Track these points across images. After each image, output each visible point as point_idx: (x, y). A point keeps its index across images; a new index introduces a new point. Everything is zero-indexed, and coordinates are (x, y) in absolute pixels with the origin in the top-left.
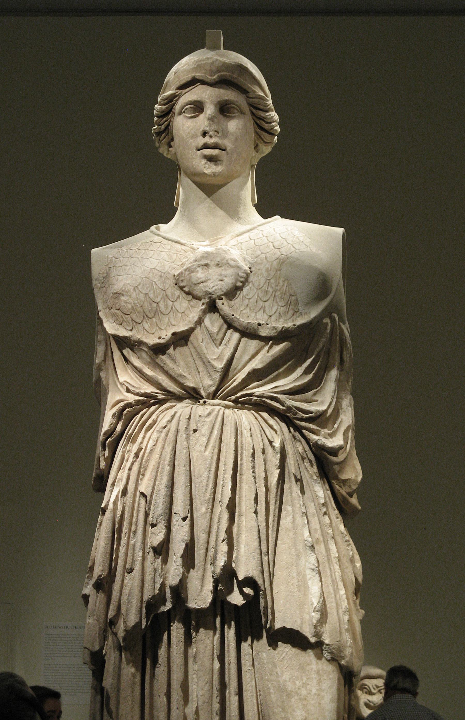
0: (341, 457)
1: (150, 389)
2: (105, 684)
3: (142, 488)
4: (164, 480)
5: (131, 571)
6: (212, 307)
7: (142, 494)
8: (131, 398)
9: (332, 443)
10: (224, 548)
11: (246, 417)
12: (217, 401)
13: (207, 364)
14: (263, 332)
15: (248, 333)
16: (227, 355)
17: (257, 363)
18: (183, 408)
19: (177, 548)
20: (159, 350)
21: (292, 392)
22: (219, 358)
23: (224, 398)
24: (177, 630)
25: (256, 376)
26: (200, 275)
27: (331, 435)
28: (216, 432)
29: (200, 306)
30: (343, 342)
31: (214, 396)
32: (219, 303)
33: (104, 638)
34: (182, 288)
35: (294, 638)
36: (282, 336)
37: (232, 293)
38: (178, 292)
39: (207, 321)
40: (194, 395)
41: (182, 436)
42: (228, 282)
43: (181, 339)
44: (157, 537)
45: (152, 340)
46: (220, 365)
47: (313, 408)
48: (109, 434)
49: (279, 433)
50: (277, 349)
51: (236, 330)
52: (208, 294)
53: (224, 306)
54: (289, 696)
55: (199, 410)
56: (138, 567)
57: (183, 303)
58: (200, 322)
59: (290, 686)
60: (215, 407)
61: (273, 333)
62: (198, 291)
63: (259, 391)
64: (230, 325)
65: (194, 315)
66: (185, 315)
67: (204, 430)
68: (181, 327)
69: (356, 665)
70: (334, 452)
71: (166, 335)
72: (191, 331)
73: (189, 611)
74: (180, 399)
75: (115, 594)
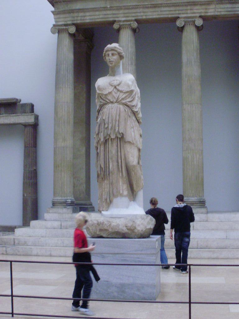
0: (138, 112)
1: (105, 102)
2: (98, 151)
3: (103, 118)
4: (107, 117)
5: (102, 132)
6: (115, 87)
7: (104, 119)
8: (102, 103)
9: (136, 110)
10: (117, 128)
11: (121, 106)
12: (116, 103)
13: (115, 98)
14: (124, 91)
15: (121, 92)
16: (118, 96)
17: (123, 97)
18: (110, 105)
19: (110, 128)
20: (106, 95)
21: (129, 102)
22: (116, 96)
23: (118, 103)
24: (110, 142)
25: (123, 99)
26: (113, 82)
27: (136, 109)
28: (116, 109)
29: (113, 88)
30: (138, 93)
31: (116, 102)
32: (116, 87)
33: (98, 144)
34: (110, 85)
35: (129, 142)
36: (127, 92)
37: (119, 85)
38: (109, 85)
39: (114, 90)
40: (112, 102)
41: (110, 109)
42: (118, 83)
43: (110, 93)
44: (106, 126)
45: (105, 93)
46: (116, 97)
47: (133, 104)
48: (98, 110)
49: (127, 109)
50: (127, 94)
51: (119, 91)
52: (114, 85)
53: (117, 87)
54: (129, 152)
55: (113, 105)
56: (103, 132)
57: (110, 87)
58: (113, 90)
59: (129, 151)
60: (116, 104)
61: (126, 92)
62: (113, 85)
63: (123, 102)
64: (118, 90)
65: (112, 89)
66: (111, 89)
67: (114, 108)
68: (110, 91)
69: (141, 148)
70: (137, 112)
71: (107, 92)
72: (112, 92)
73: (111, 139)
74: (110, 103)
75: (99, 136)
